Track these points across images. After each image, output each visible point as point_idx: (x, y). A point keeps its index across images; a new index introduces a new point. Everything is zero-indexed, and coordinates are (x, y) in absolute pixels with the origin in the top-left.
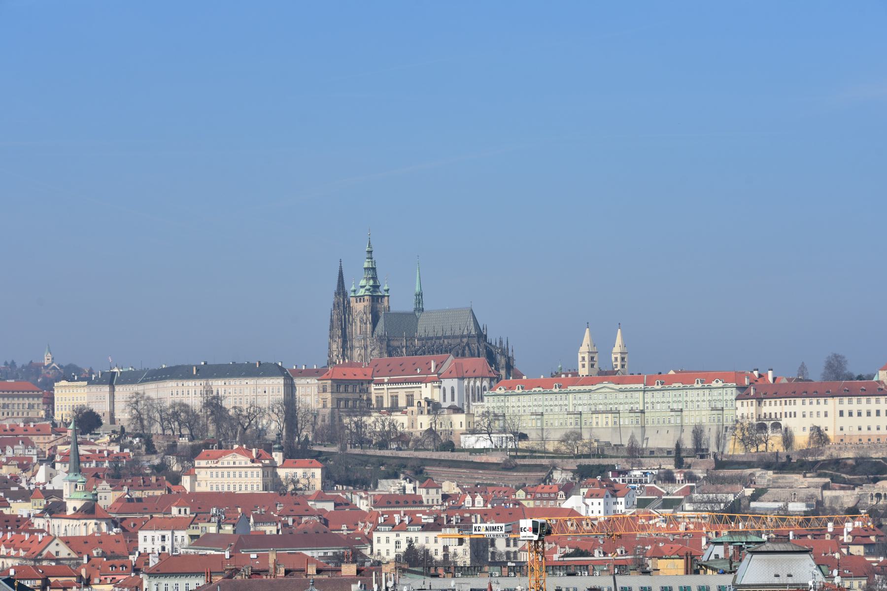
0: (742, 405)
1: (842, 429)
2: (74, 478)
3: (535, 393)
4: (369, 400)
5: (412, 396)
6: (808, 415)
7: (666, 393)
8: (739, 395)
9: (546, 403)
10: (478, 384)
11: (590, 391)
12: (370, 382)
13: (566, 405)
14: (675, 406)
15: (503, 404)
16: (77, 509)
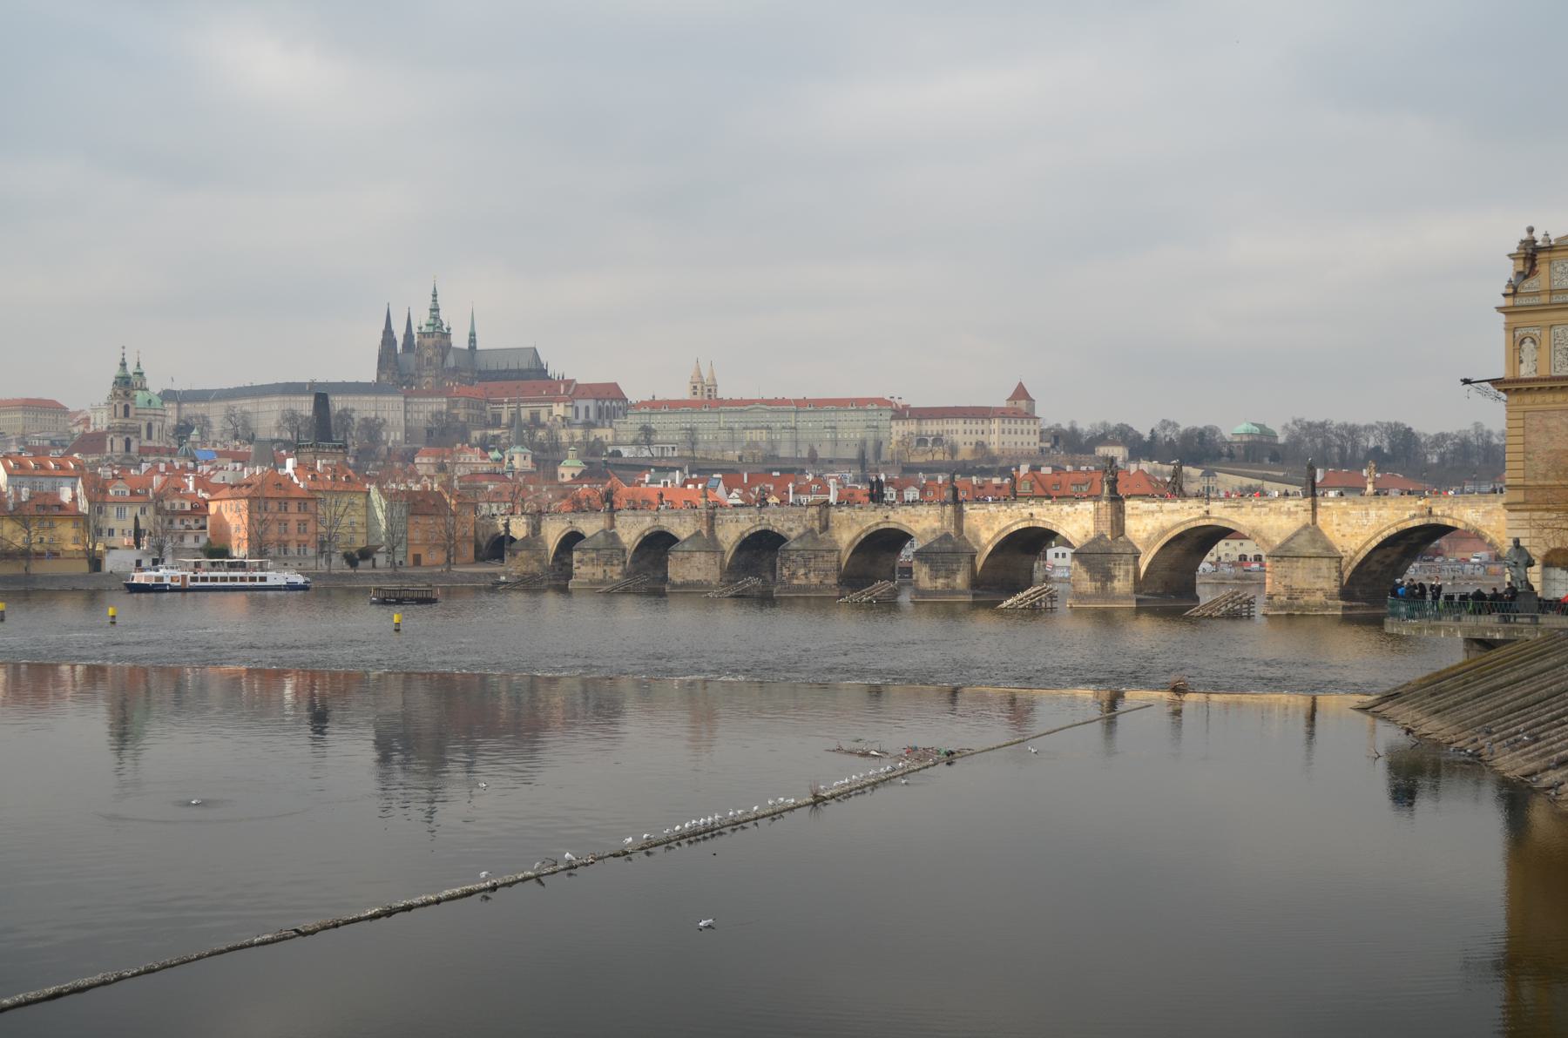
0: (897, 424)
1: (1003, 443)
2: (523, 450)
3: (683, 412)
4: (486, 417)
5: (539, 413)
6: (968, 432)
7: (817, 414)
8: (892, 416)
9: (694, 420)
10: (614, 404)
11: (741, 411)
12: (488, 401)
13: (716, 422)
14: (827, 424)
15: (648, 421)
16: (576, 475)
